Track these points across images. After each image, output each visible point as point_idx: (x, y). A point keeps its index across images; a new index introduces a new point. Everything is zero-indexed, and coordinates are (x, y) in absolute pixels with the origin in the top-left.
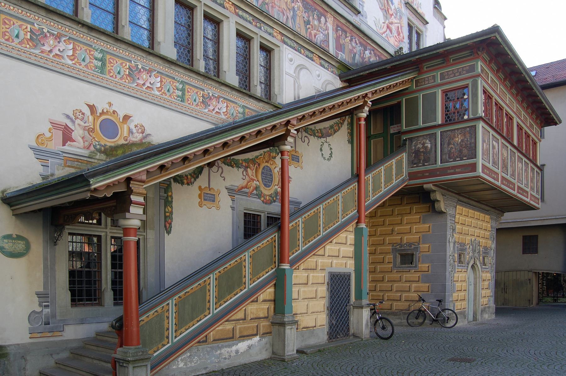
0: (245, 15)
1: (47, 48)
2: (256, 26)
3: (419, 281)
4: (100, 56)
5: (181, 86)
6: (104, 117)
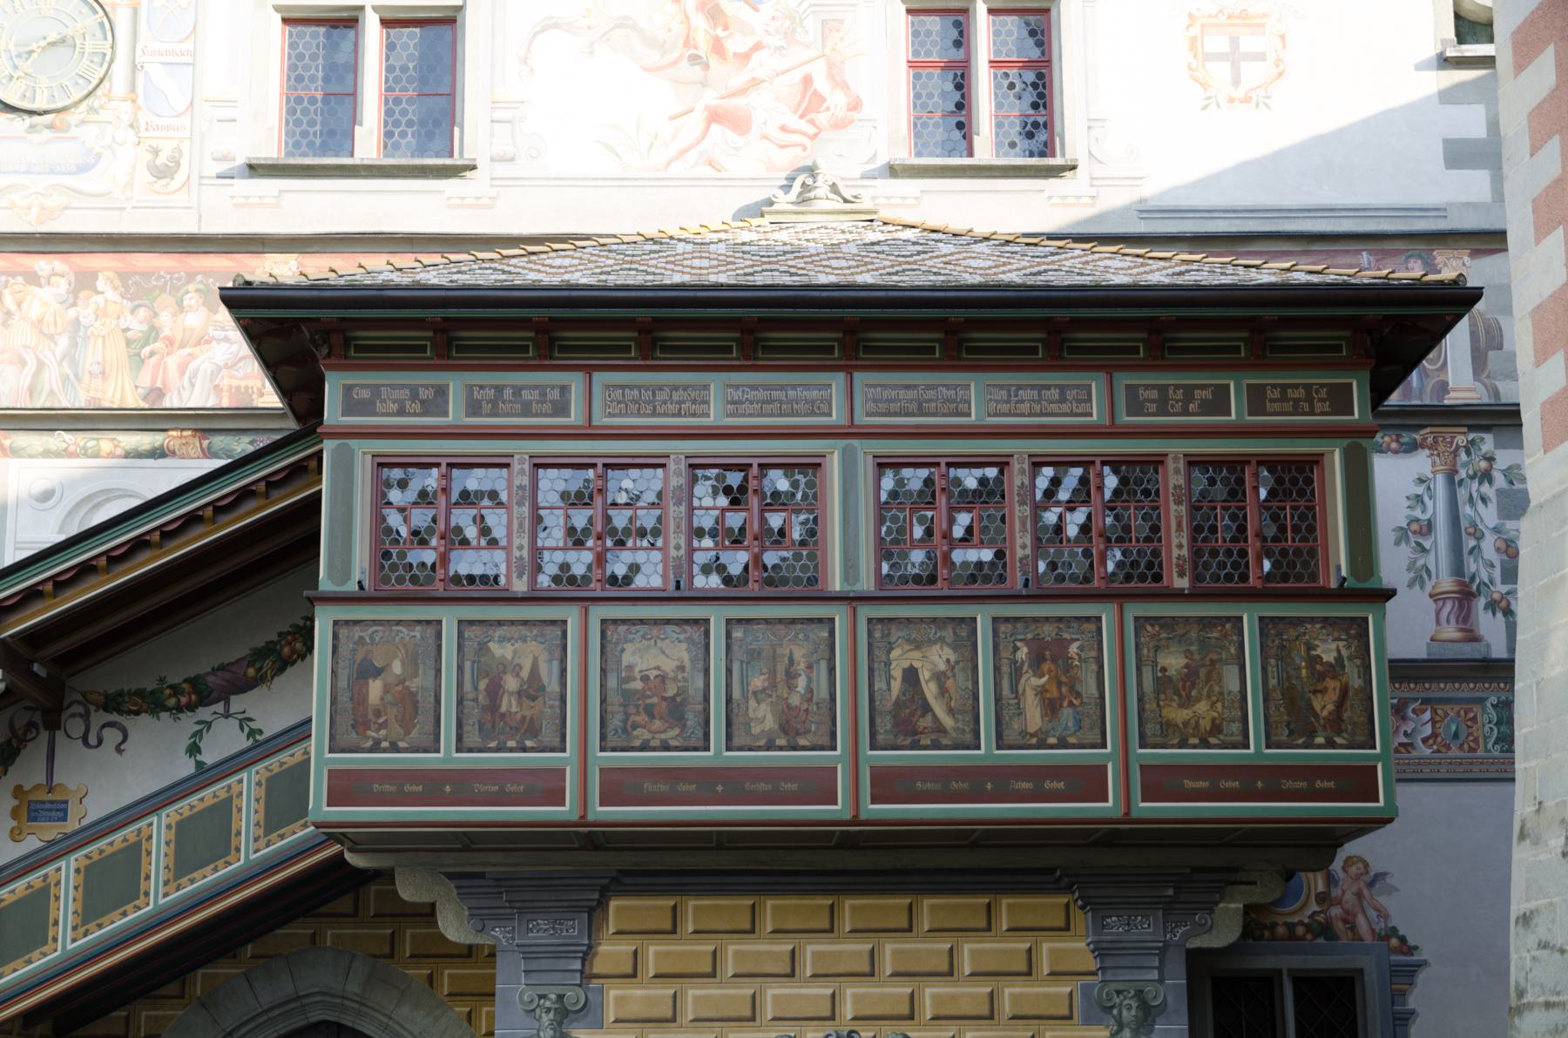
3: (1070, 1017)
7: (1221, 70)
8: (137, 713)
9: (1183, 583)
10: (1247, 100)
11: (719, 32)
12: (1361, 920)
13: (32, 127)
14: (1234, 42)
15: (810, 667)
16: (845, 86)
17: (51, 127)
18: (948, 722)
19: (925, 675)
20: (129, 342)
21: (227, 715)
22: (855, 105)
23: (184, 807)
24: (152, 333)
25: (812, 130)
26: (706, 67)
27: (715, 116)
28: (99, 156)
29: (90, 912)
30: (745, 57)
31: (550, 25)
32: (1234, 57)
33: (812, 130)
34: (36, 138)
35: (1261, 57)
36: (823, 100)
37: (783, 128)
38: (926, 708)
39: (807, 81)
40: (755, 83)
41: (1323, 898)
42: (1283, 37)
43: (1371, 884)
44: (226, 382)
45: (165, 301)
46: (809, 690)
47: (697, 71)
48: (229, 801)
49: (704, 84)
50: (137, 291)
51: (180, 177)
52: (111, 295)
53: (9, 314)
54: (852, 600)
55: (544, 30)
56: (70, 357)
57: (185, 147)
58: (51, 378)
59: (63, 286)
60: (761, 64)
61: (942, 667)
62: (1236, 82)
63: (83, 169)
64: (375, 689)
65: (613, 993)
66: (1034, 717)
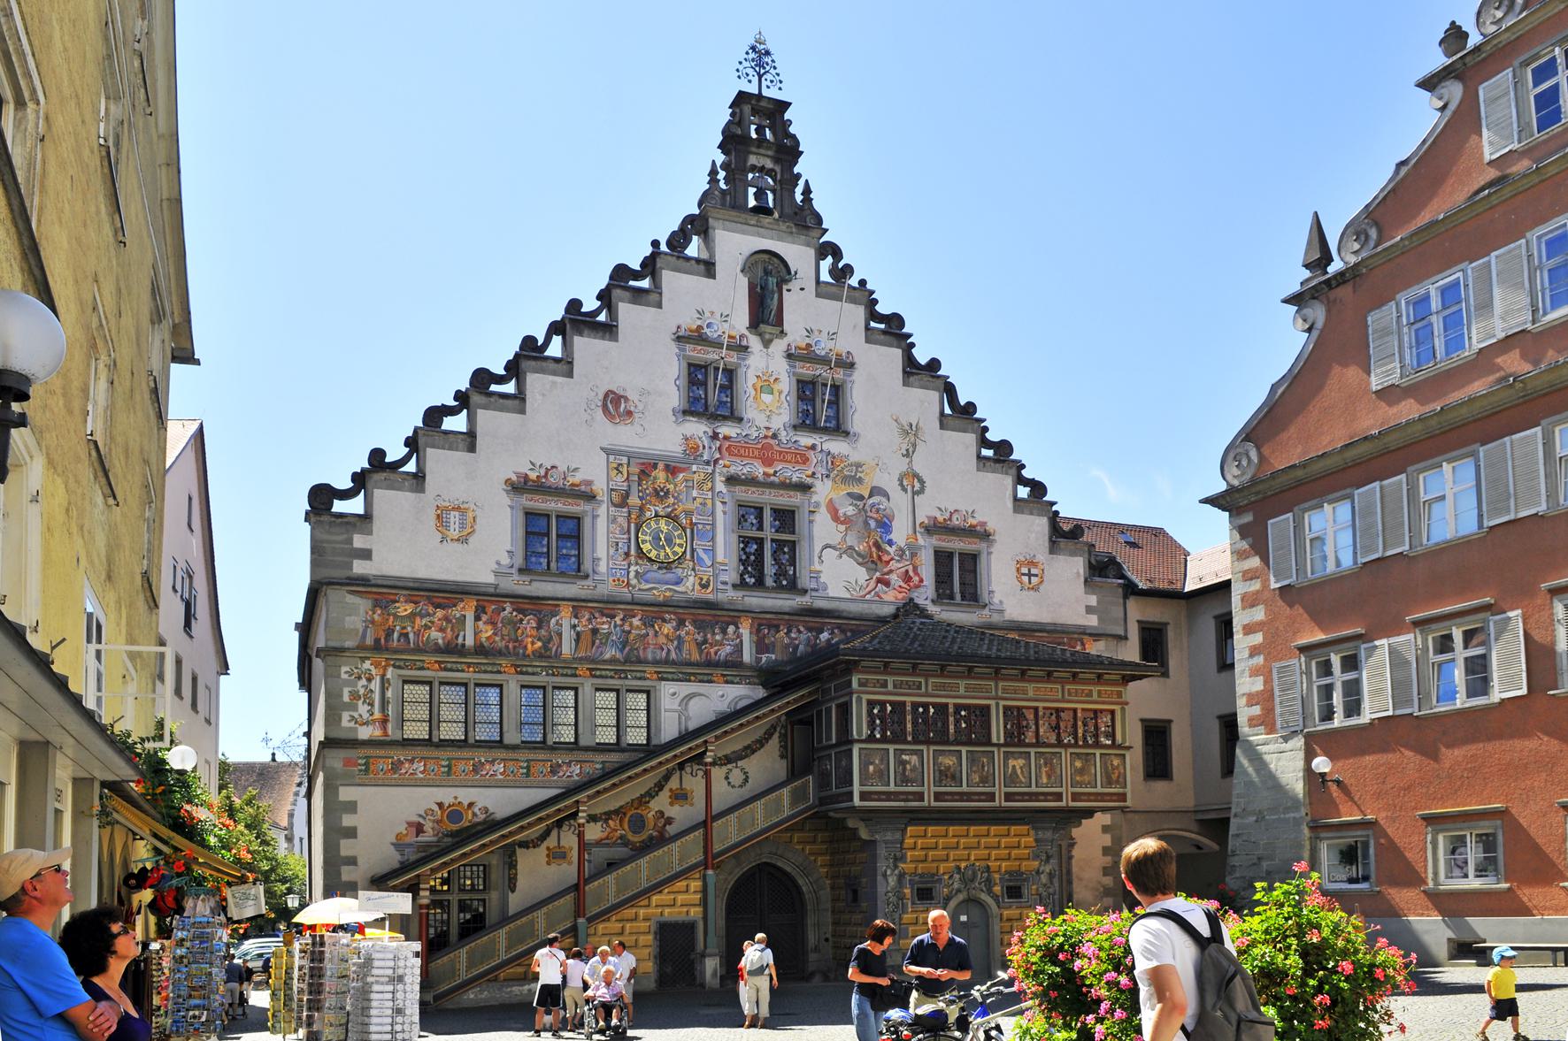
0: (604, 673)
1: (403, 771)
2: (620, 678)
13: (659, 568)
17: (666, 568)
20: (697, 644)
24: (705, 641)
27: (879, 581)
30: (888, 563)
31: (827, 546)
34: (661, 572)
39: (907, 571)
40: (891, 571)
45: (709, 630)
47: (873, 566)
49: (876, 570)
50: (700, 625)
51: (710, 589)
53: (656, 632)
56: (679, 648)
59: (675, 624)
60: (893, 565)
63: (677, 583)
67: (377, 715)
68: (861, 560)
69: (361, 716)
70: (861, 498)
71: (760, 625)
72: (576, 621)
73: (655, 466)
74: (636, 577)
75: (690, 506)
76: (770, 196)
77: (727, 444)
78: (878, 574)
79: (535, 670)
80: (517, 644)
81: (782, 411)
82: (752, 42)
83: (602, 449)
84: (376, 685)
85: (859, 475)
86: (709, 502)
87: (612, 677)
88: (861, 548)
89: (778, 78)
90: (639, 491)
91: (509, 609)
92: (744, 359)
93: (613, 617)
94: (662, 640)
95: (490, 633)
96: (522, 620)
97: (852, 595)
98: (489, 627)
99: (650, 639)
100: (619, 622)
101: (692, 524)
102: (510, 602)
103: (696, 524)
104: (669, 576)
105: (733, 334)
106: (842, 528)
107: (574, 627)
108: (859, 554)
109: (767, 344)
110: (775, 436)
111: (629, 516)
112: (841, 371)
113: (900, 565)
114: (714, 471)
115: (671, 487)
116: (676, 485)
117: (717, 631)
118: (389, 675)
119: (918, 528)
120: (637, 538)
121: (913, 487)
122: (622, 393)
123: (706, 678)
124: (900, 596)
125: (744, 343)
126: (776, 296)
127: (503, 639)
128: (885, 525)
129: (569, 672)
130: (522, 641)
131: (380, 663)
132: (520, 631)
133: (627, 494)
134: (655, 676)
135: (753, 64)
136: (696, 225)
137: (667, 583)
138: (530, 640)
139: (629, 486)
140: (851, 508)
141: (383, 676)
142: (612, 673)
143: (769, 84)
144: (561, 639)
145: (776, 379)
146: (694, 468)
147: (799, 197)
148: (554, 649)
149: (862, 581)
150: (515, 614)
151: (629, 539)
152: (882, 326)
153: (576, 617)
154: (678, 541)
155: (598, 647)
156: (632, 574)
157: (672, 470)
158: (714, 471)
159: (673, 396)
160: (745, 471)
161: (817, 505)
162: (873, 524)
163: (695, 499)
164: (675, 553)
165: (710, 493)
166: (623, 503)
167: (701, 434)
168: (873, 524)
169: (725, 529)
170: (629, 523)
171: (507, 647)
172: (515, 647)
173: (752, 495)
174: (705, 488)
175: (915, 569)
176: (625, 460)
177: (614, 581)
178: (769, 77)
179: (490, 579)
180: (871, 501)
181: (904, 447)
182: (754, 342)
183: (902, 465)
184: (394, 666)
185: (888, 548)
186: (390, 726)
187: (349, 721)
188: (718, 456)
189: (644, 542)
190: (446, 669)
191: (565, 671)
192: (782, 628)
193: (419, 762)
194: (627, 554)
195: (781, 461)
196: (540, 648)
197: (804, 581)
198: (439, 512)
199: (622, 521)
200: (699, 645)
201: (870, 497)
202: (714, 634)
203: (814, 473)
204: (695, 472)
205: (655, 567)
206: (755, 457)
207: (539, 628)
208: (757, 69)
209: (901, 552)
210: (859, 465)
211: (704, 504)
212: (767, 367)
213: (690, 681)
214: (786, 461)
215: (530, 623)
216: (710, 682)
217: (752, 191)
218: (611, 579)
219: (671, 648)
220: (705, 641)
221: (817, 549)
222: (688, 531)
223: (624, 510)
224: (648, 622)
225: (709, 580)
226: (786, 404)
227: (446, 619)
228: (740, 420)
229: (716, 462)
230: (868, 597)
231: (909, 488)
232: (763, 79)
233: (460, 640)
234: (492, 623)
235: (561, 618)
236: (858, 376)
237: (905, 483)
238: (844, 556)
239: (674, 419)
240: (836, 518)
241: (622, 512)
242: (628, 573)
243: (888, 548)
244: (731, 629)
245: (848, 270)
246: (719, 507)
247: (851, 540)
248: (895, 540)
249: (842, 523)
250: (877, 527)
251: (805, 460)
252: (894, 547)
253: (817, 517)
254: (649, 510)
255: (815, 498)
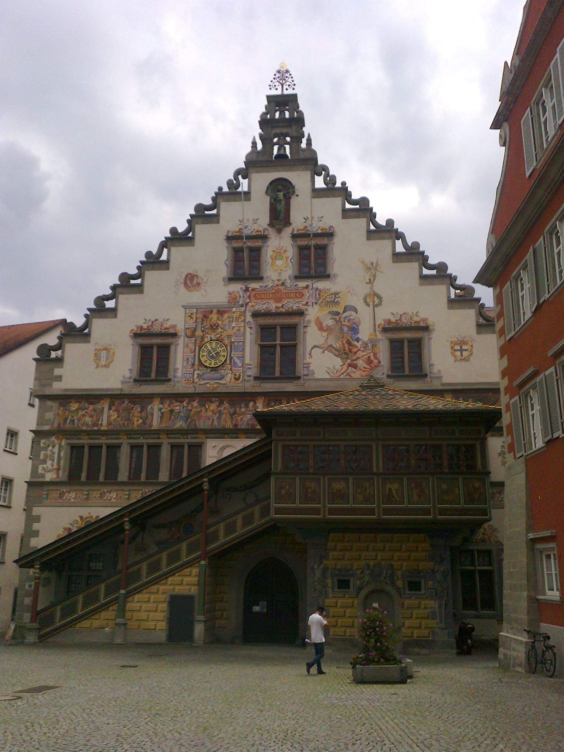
2: (184, 438)
4: (86, 493)
5: (128, 493)
6: (87, 520)
7: (458, 353)
8: (233, 491)
9: (446, 471)
10: (464, 360)
11: (351, 347)
12: (492, 539)
13: (211, 371)
14: (461, 347)
15: (370, 488)
16: (377, 359)
17: (215, 370)
18: (398, 499)
19: (393, 490)
20: (230, 415)
21: (251, 492)
22: (379, 362)
23: (245, 513)
24: (235, 413)
25: (370, 368)
26: (348, 355)
27: (350, 365)
28: (224, 376)
29: (227, 534)
30: (356, 353)
31: (315, 347)
32: (461, 350)
33: (370, 368)
34: (212, 373)
35: (467, 350)
36: (373, 361)
37: (364, 367)
38: (393, 496)
39: (369, 357)
40: (358, 358)
41: (483, 534)
42: (472, 346)
43: (494, 531)
44: (250, 423)
46: (370, 492)
47: (345, 356)
48: (253, 512)
49: (348, 359)
50: (232, 404)
51: (241, 380)
52: (227, 405)
54: (378, 474)
55: (314, 348)
56: (219, 418)
57: (241, 374)
58: (216, 423)
59: (217, 403)
60: (360, 354)
61: (396, 488)
62: (462, 355)
63: (221, 379)
64: (283, 492)
65: (331, 554)
66: (416, 498)
67: (55, 466)
68: (337, 353)
69: (47, 467)
70: (338, 313)
71: (269, 400)
72: (161, 406)
73: (211, 312)
74: (198, 377)
75: (230, 332)
76: (287, 147)
77: (254, 293)
78: (349, 361)
79: (137, 436)
80: (129, 422)
81: (288, 269)
82: (278, 68)
83: (183, 306)
84: (56, 450)
85: (336, 299)
86: (242, 329)
87: (179, 438)
88: (338, 345)
89: (293, 83)
90: (202, 327)
91: (126, 402)
92: (266, 242)
93: (182, 402)
94: (209, 414)
95: (116, 416)
96: (133, 408)
97: (331, 376)
98: (116, 413)
99: (203, 414)
100: (185, 405)
101: (231, 342)
102: (128, 398)
103: (234, 342)
104: (217, 375)
105: (260, 229)
106: (325, 334)
107: (160, 409)
108: (336, 350)
109: (279, 231)
110: (283, 284)
111: (196, 342)
112: (326, 239)
113: (365, 353)
114: (245, 310)
115: (220, 322)
116: (223, 321)
117: (243, 406)
118: (63, 444)
119: (377, 328)
120: (199, 354)
121: (374, 302)
122: (194, 273)
123: (234, 436)
124: (364, 374)
125: (266, 233)
126: (283, 202)
127: (122, 420)
128: (354, 329)
129: (156, 436)
130: (132, 420)
131: (59, 437)
132: (131, 414)
133: (195, 330)
134: (204, 436)
135: (278, 79)
136: (243, 173)
137: (215, 379)
138: (136, 419)
139: (196, 326)
140: (331, 321)
141: (60, 444)
142: (180, 436)
143: (287, 87)
144: (152, 418)
145: (285, 251)
146: (234, 310)
147: (304, 145)
148: (148, 424)
149: (338, 367)
150: (129, 404)
151: (195, 356)
152: (358, 206)
153: (162, 404)
154: (222, 354)
155: (173, 421)
156: (195, 376)
157: (221, 313)
158: (245, 310)
159: (224, 271)
160: (264, 307)
161: (309, 321)
162: (345, 329)
163: (234, 328)
164: (220, 361)
165: (243, 324)
166: (193, 335)
167: (239, 290)
168: (345, 329)
169: (251, 343)
170: (195, 346)
171: (124, 424)
172: (128, 424)
173: (269, 321)
174: (240, 320)
175: (375, 355)
176: (195, 310)
177: (185, 381)
178: (288, 83)
179: (118, 385)
180: (344, 315)
181: (368, 278)
182: (271, 233)
183: (366, 289)
184: (66, 438)
185: (356, 343)
186: (61, 472)
187: (42, 470)
188: (248, 300)
189: (203, 356)
190: (91, 439)
191: (153, 436)
192: (283, 401)
193: (73, 492)
194: (193, 365)
195: (287, 298)
196: (141, 423)
197: (300, 370)
198: (96, 352)
199: (191, 346)
200: (231, 415)
201: (344, 312)
202: (241, 408)
203: (307, 303)
204: (234, 312)
205: (209, 370)
206: (270, 299)
207: (141, 412)
208: (281, 81)
209: (365, 345)
210: (336, 294)
211: (239, 330)
212: (279, 245)
213: (224, 438)
214: (290, 298)
215: (137, 409)
216: (236, 438)
217: (276, 148)
218: (184, 380)
219: (215, 418)
220: (235, 413)
221: (308, 349)
222: (229, 347)
223: (193, 339)
224: (202, 404)
225: (240, 375)
226: (290, 264)
227: (94, 410)
228: (261, 278)
229: (247, 304)
230: (342, 376)
231: (371, 304)
232: (284, 86)
233: (100, 422)
234: (117, 411)
235: (154, 405)
236: (336, 239)
237: (368, 300)
238: (326, 352)
239: (223, 283)
240: (321, 328)
241: (192, 340)
242: (193, 376)
243: (356, 343)
244: (251, 404)
245: (333, 178)
246: (248, 330)
247: (331, 341)
248: (361, 338)
249: (325, 331)
250: (348, 331)
251: (302, 295)
252: (360, 342)
253: (309, 330)
254: (207, 337)
255: (307, 318)
